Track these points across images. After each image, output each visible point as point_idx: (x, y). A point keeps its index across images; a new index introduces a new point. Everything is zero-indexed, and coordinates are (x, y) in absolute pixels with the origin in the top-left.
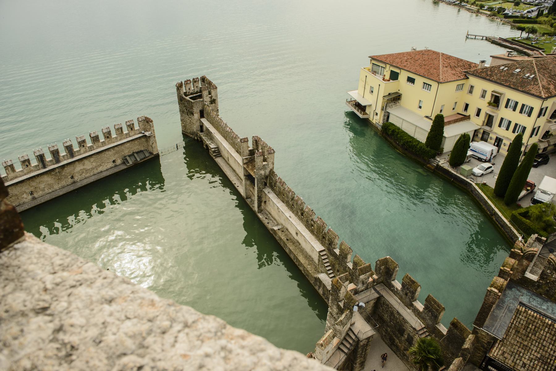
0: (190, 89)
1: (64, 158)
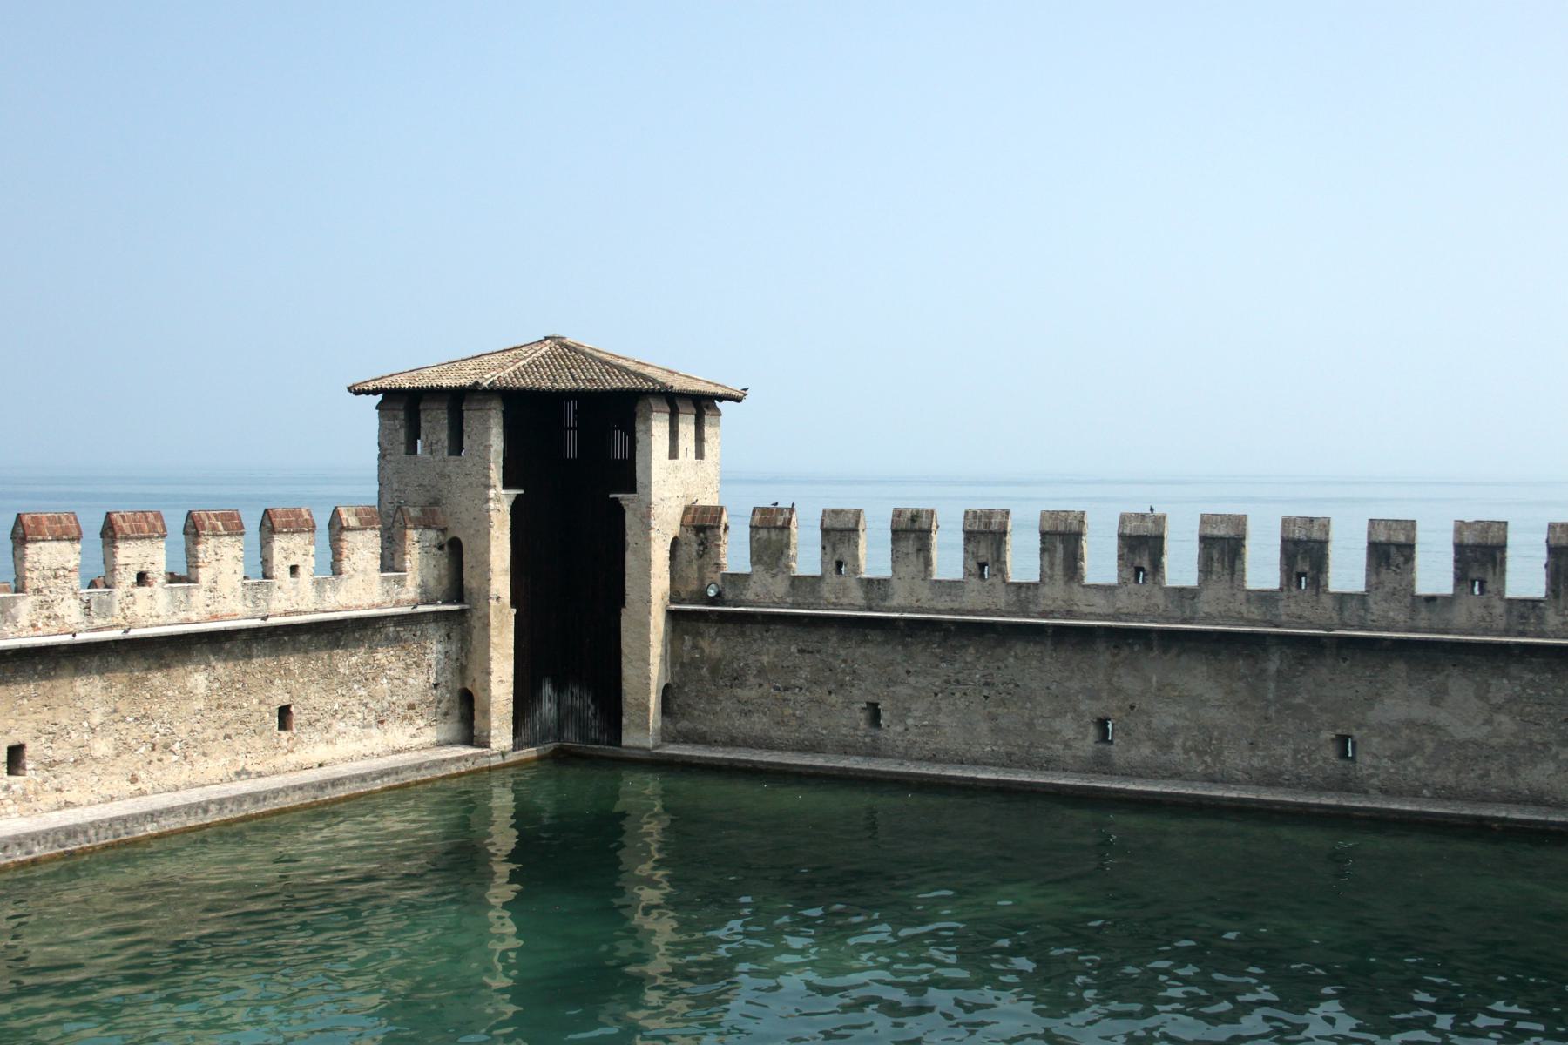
1: (1341, 611)
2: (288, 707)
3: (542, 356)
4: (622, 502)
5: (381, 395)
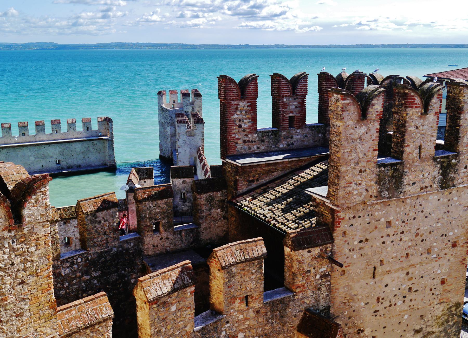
0: (175, 101)
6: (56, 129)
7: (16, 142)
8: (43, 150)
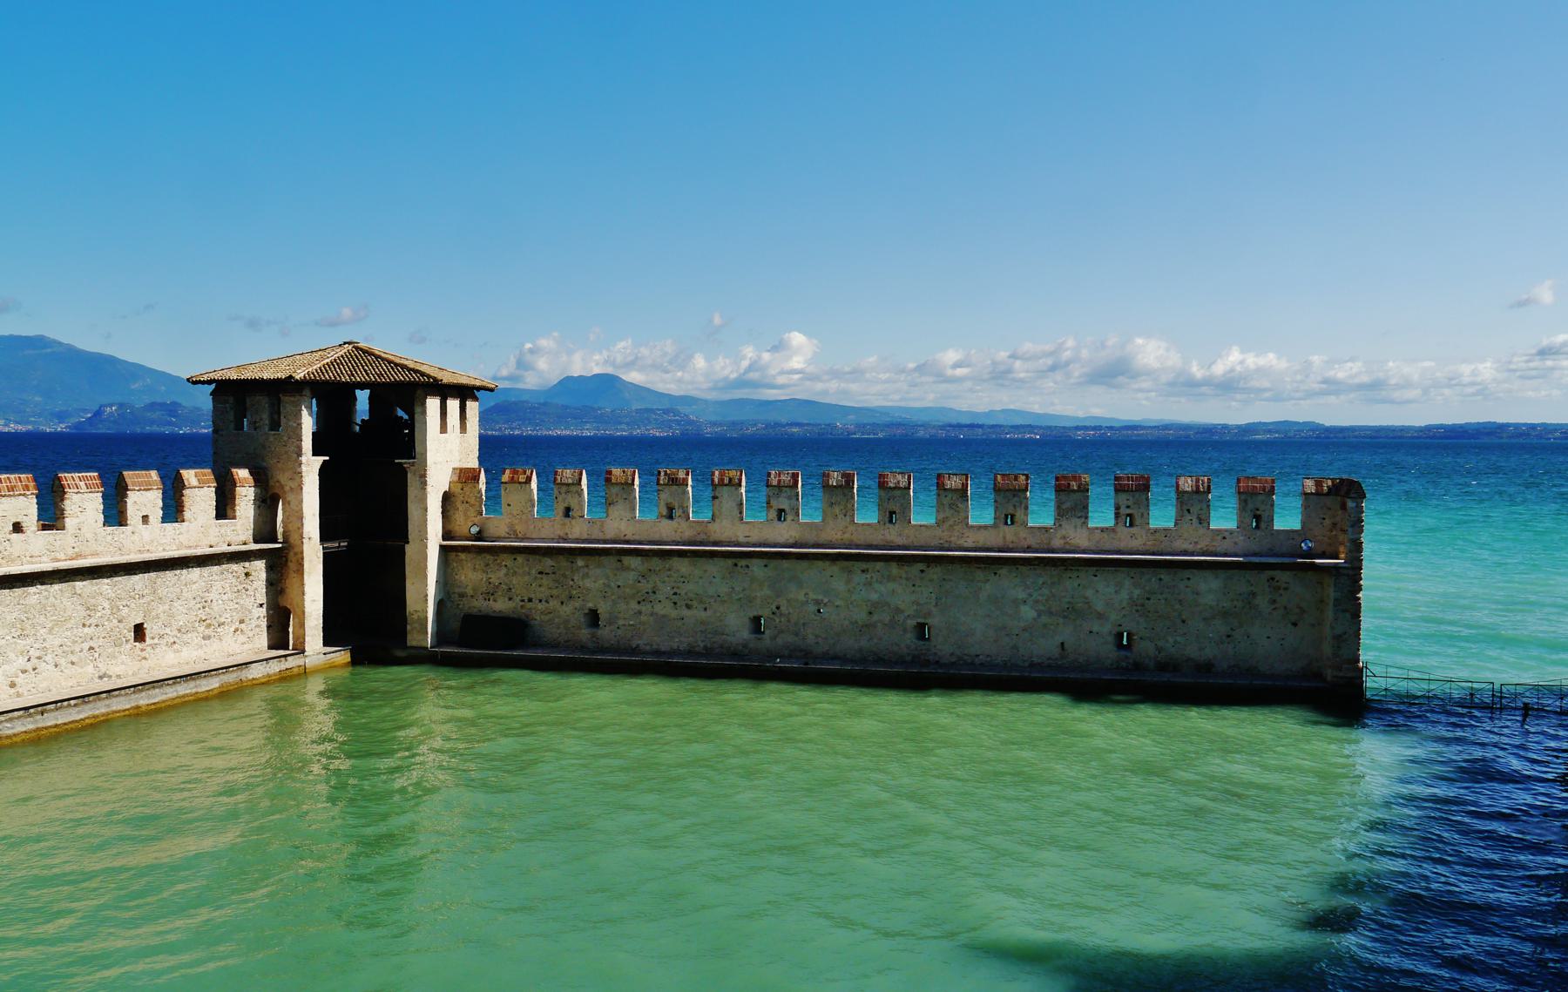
2: (142, 624)
3: (342, 356)
4: (405, 466)
5: (213, 386)
6: (1128, 511)
7: (980, 545)
8: (1071, 585)
